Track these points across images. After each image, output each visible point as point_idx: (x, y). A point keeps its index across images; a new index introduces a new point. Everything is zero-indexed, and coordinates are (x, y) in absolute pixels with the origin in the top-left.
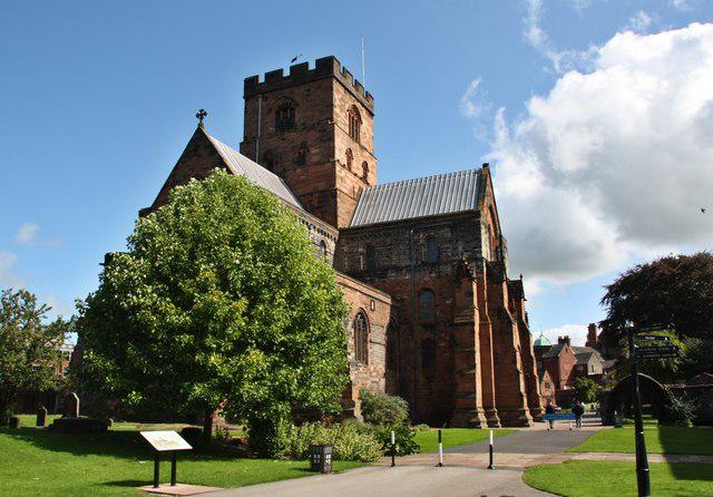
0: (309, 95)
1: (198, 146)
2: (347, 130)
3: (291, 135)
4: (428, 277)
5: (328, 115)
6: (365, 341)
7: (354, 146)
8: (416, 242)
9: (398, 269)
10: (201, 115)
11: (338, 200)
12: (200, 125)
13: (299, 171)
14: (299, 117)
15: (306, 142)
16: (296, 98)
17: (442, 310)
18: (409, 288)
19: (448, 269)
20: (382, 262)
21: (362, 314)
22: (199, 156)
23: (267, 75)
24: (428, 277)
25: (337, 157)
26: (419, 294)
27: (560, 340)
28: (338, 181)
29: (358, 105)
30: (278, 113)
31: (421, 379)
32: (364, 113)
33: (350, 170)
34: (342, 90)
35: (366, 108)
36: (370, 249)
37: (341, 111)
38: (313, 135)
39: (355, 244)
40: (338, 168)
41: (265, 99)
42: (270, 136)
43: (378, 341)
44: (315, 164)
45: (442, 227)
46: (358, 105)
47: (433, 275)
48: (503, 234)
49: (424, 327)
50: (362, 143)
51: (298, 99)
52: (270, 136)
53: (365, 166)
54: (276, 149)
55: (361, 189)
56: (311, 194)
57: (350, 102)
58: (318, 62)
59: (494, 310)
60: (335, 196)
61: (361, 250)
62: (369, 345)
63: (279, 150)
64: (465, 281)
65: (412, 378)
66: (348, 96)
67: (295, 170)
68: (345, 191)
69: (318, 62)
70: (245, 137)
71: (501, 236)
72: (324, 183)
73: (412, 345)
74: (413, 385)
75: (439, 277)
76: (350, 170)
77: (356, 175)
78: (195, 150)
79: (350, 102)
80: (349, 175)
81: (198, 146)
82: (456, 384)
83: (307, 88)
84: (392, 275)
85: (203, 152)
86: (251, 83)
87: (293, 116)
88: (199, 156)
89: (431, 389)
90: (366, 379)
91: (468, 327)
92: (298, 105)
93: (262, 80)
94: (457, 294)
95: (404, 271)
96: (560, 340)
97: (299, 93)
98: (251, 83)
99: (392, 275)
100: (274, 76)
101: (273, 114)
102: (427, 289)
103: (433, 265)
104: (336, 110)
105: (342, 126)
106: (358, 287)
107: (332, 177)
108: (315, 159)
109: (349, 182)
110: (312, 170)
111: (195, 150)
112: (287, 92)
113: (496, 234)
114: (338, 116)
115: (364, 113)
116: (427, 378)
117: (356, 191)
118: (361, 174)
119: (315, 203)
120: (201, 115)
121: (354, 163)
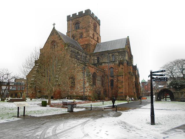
0: (83, 20)
1: (53, 33)
3: (80, 31)
4: (112, 65)
7: (95, 33)
8: (109, 56)
9: (104, 63)
10: (54, 24)
12: (54, 27)
13: (81, 39)
14: (80, 25)
16: (79, 20)
19: (117, 62)
20: (101, 61)
21: (94, 73)
23: (73, 15)
24: (112, 65)
26: (110, 69)
28: (91, 42)
29: (96, 22)
30: (75, 25)
31: (110, 89)
32: (98, 24)
33: (94, 39)
36: (98, 58)
38: (84, 30)
41: (72, 21)
43: (99, 80)
46: (96, 22)
56: (84, 45)
57: (94, 22)
58: (85, 11)
61: (96, 58)
64: (121, 66)
68: (92, 44)
69: (85, 11)
70: (68, 31)
72: (87, 42)
75: (115, 65)
76: (94, 39)
77: (95, 40)
78: (53, 34)
79: (94, 22)
82: (118, 90)
84: (103, 64)
85: (55, 34)
86: (68, 17)
88: (54, 35)
90: (96, 89)
92: (80, 22)
93: (71, 16)
94: (119, 69)
95: (106, 63)
97: (80, 19)
98: (68, 17)
99: (103, 64)
100: (74, 15)
102: (112, 68)
103: (114, 62)
108: (85, 36)
109: (93, 42)
110: (84, 39)
113: (130, 54)
114: (91, 25)
115: (98, 24)
118: (96, 40)
119: (85, 47)
120: (54, 24)
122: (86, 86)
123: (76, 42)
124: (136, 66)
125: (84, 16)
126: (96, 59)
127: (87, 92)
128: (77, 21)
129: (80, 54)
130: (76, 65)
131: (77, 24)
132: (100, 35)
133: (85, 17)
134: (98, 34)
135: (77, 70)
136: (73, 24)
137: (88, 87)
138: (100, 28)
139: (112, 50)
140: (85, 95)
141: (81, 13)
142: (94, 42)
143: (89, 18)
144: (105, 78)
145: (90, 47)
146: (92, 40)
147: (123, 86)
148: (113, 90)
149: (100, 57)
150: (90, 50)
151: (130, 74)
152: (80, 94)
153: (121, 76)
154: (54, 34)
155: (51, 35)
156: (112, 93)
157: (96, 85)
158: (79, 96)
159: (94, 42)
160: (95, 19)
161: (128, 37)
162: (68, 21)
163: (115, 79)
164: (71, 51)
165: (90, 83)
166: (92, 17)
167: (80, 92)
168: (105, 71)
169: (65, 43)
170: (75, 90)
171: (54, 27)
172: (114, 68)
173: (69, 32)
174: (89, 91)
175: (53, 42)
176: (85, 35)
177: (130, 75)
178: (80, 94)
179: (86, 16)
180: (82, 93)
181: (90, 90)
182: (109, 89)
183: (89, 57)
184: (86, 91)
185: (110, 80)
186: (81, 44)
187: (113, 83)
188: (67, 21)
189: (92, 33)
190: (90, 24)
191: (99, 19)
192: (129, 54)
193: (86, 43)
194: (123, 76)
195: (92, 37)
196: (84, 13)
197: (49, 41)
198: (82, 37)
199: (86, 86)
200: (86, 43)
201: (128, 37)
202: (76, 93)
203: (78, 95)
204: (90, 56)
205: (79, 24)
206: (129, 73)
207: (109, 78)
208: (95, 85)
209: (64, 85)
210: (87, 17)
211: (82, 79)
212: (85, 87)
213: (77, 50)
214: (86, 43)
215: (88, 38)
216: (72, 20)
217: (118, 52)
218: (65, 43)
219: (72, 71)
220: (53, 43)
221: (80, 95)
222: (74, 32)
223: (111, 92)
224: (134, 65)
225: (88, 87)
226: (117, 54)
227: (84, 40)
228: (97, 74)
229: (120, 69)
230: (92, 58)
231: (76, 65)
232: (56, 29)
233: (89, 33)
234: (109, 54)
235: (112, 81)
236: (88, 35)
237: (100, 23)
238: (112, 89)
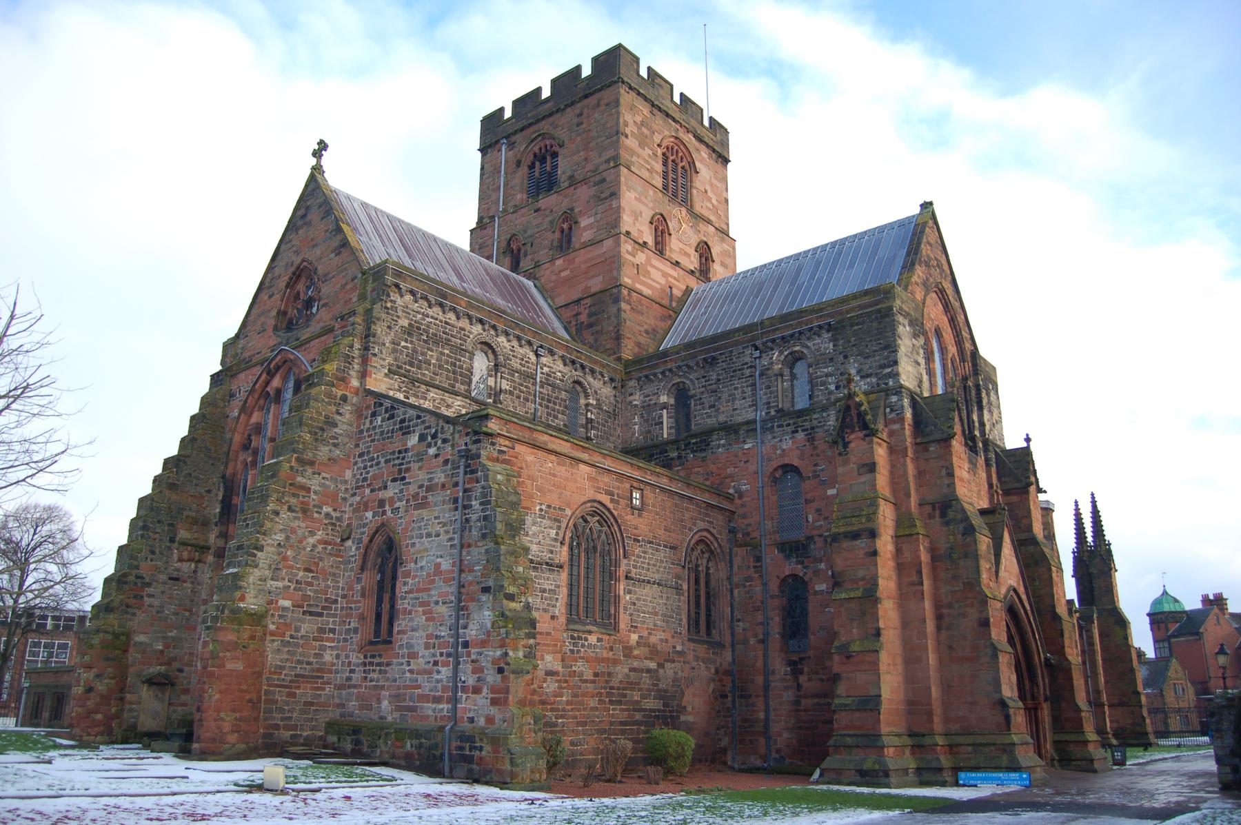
2: (658, 181)
3: (549, 201)
4: (788, 446)
5: (610, 153)
6: (610, 575)
11: (623, 305)
12: (317, 170)
13: (559, 262)
14: (564, 166)
15: (572, 209)
17: (818, 511)
18: (752, 468)
20: (702, 419)
22: (309, 224)
23: (518, 104)
24: (788, 446)
25: (627, 223)
27: (1205, 600)
29: (689, 139)
30: (532, 166)
32: (702, 157)
34: (645, 109)
35: (707, 146)
37: (642, 145)
39: (649, 389)
40: (626, 247)
41: (511, 146)
42: (517, 209)
44: (585, 246)
45: (816, 332)
46: (689, 139)
47: (801, 436)
48: (984, 352)
49: (782, 550)
50: (698, 208)
51: (561, 134)
52: (517, 209)
53: (704, 252)
54: (525, 231)
55: (688, 291)
56: (578, 301)
57: (663, 132)
58: (596, 61)
59: (933, 505)
60: (617, 300)
61: (664, 399)
62: (622, 586)
63: (529, 232)
64: (855, 439)
65: (760, 664)
66: (659, 120)
67: (553, 260)
68: (647, 292)
71: (975, 353)
72: (601, 278)
73: (758, 589)
74: (760, 680)
78: (304, 216)
79: (663, 132)
80: (656, 261)
81: (308, 208)
83: (578, 111)
84: (719, 441)
85: (314, 216)
86: (492, 123)
87: (555, 167)
88: (309, 224)
89: (799, 687)
90: (615, 662)
91: (861, 543)
96: (1205, 600)
101: (524, 170)
102: (788, 468)
103: (801, 413)
104: (631, 142)
105: (645, 174)
106: (585, 456)
107: (613, 262)
108: (586, 236)
109: (655, 274)
110: (581, 257)
111: (304, 216)
112: (544, 126)
113: (961, 350)
114: (632, 153)
115: (702, 157)
116: (791, 663)
117: (677, 293)
118: (692, 262)
119: (583, 318)
121: (674, 245)
122: (472, 632)
123: (529, 284)
124: (1023, 458)
125: (586, 97)
126: (664, 406)
127: (477, 690)
128: (543, 136)
129: (515, 364)
130: (413, 440)
131: (543, 160)
132: (724, 232)
133: (591, 101)
134: (709, 222)
135: (418, 475)
136: (519, 164)
137: (483, 644)
138: (724, 180)
139: (784, 318)
140: (466, 726)
141: (567, 83)
142: (665, 275)
143: (617, 103)
144: (737, 561)
145: (619, 310)
146: (641, 257)
147: (878, 633)
148: (803, 679)
149: (695, 389)
150: (618, 338)
151: (951, 514)
152: (429, 708)
153: (855, 536)
154: (309, 217)
155: (293, 226)
156: (797, 703)
157: (616, 628)
158: (416, 734)
159: (665, 275)
160: (677, 116)
161: (927, 206)
162: (483, 150)
163: (817, 573)
164: (409, 331)
165: (511, 597)
166: (646, 99)
167: (426, 687)
168: (729, 498)
169: (364, 273)
170: (394, 671)
171: (317, 170)
172: (807, 471)
173: (486, 220)
174: (492, 677)
175: (302, 273)
176: (586, 229)
177: (947, 523)
178: (429, 708)
179: (598, 96)
180: (437, 700)
181: (501, 671)
182: (767, 672)
183: (606, 391)
184: (471, 681)
185: (774, 586)
186: (561, 301)
187: (804, 614)
188: (479, 154)
189: (647, 215)
190: (627, 149)
191: (711, 119)
192: (952, 350)
193: (596, 284)
194: (873, 534)
195: (650, 240)
196: (588, 78)
197: (277, 271)
198: (569, 241)
199: (472, 632)
200: (590, 283)
201: (927, 206)
202: (397, 698)
203: (412, 722)
204: (620, 385)
205: (555, 155)
206: (943, 514)
207: (767, 560)
208: (609, 624)
209: (308, 627)
210: (602, 103)
211: (446, 565)
212: (466, 645)
213: (477, 329)
214: (590, 283)
215: (608, 243)
216: (513, 139)
217: (830, 328)
218: (364, 273)
219: (382, 494)
220: (300, 286)
221: (420, 725)
222: (520, 221)
223: (789, 695)
224: (1012, 441)
225: (483, 644)
226: (824, 344)
227: (583, 267)
228: (631, 519)
229: (847, 469)
230: (637, 399)
231: (413, 440)
232: (337, 178)
233: (619, 209)
234: (765, 350)
235: (795, 590)
236: (611, 227)
237: (725, 144)
238: (795, 667)
